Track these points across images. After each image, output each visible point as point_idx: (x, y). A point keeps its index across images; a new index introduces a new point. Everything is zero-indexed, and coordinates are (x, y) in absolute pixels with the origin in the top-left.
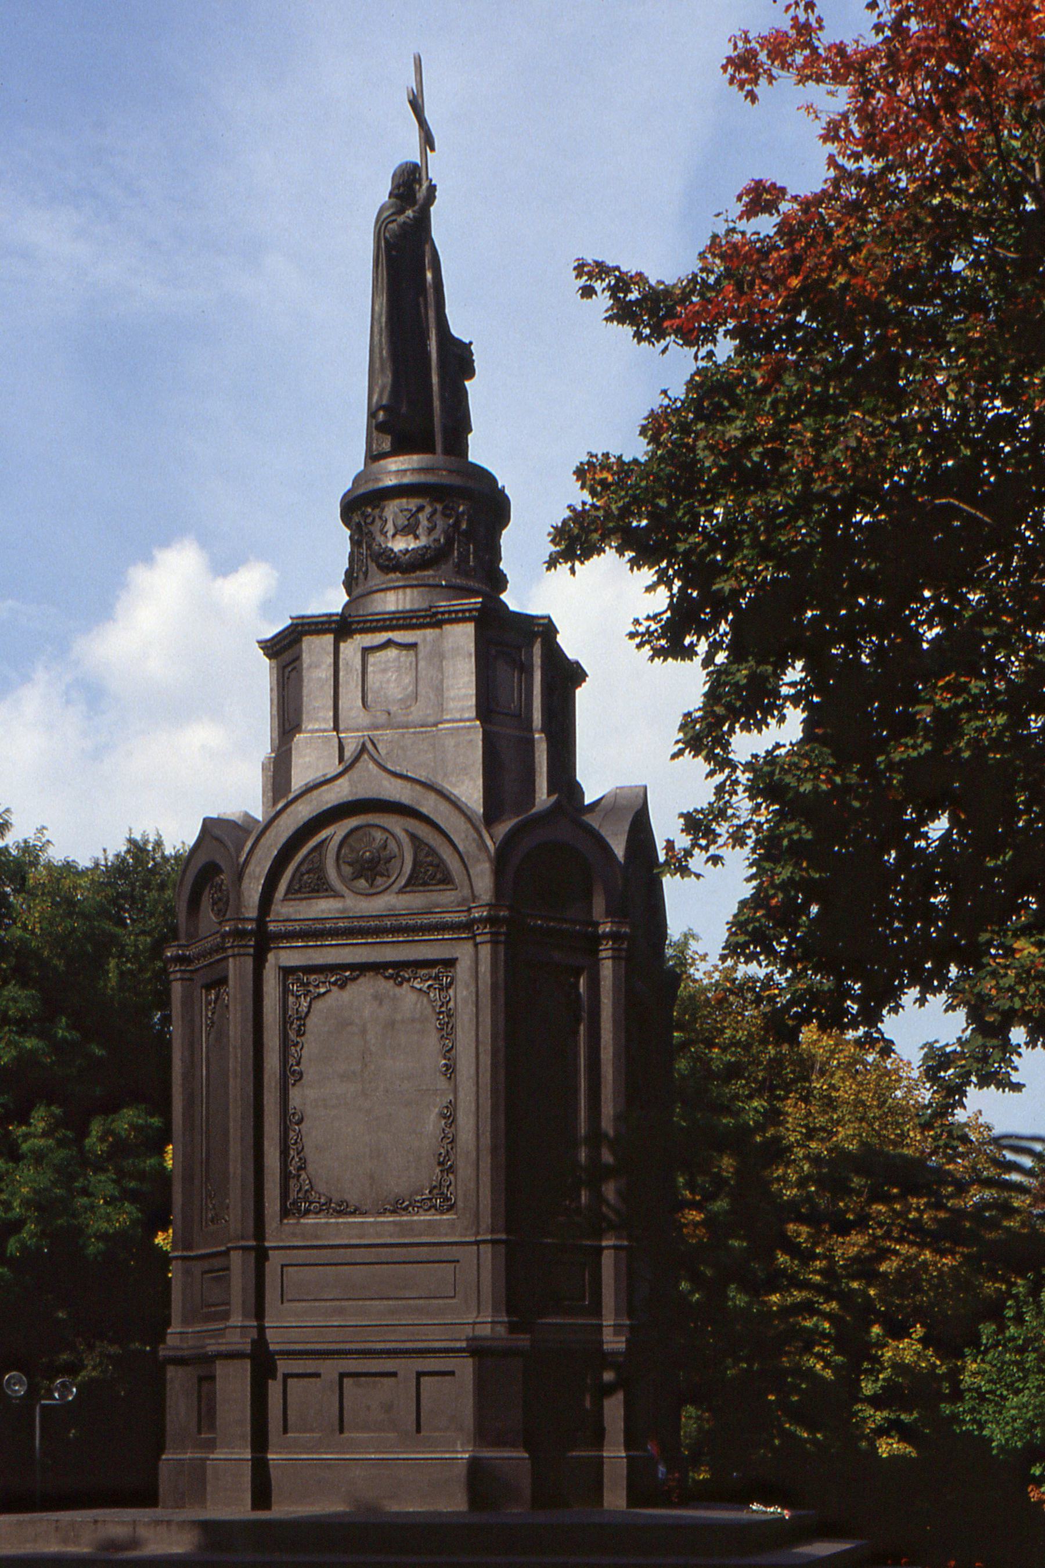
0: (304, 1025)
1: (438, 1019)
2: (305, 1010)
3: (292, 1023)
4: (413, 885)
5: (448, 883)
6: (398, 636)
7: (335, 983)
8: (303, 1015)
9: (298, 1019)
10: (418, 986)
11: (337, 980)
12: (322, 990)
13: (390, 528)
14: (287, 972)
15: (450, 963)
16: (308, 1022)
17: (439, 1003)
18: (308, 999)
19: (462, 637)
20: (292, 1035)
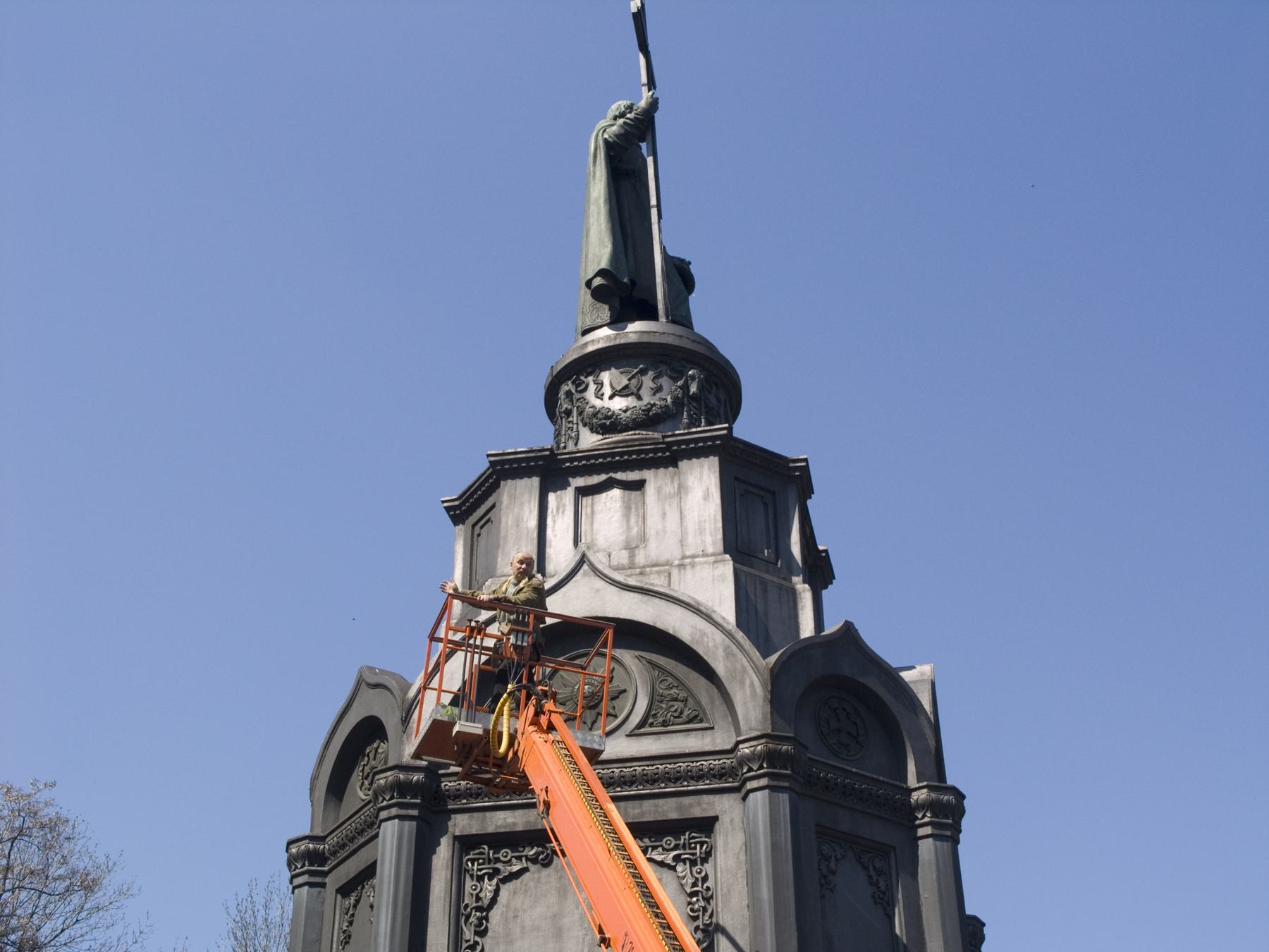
0: (487, 919)
1: (690, 903)
2: (490, 895)
3: (468, 917)
4: (651, 725)
5: (701, 721)
6: (620, 476)
7: (534, 860)
8: (486, 902)
9: (478, 909)
10: (659, 858)
11: (538, 854)
12: (515, 868)
13: (607, 391)
14: (466, 844)
15: (707, 825)
16: (495, 915)
17: (691, 881)
18: (495, 881)
19: (701, 483)
20: (468, 934)
